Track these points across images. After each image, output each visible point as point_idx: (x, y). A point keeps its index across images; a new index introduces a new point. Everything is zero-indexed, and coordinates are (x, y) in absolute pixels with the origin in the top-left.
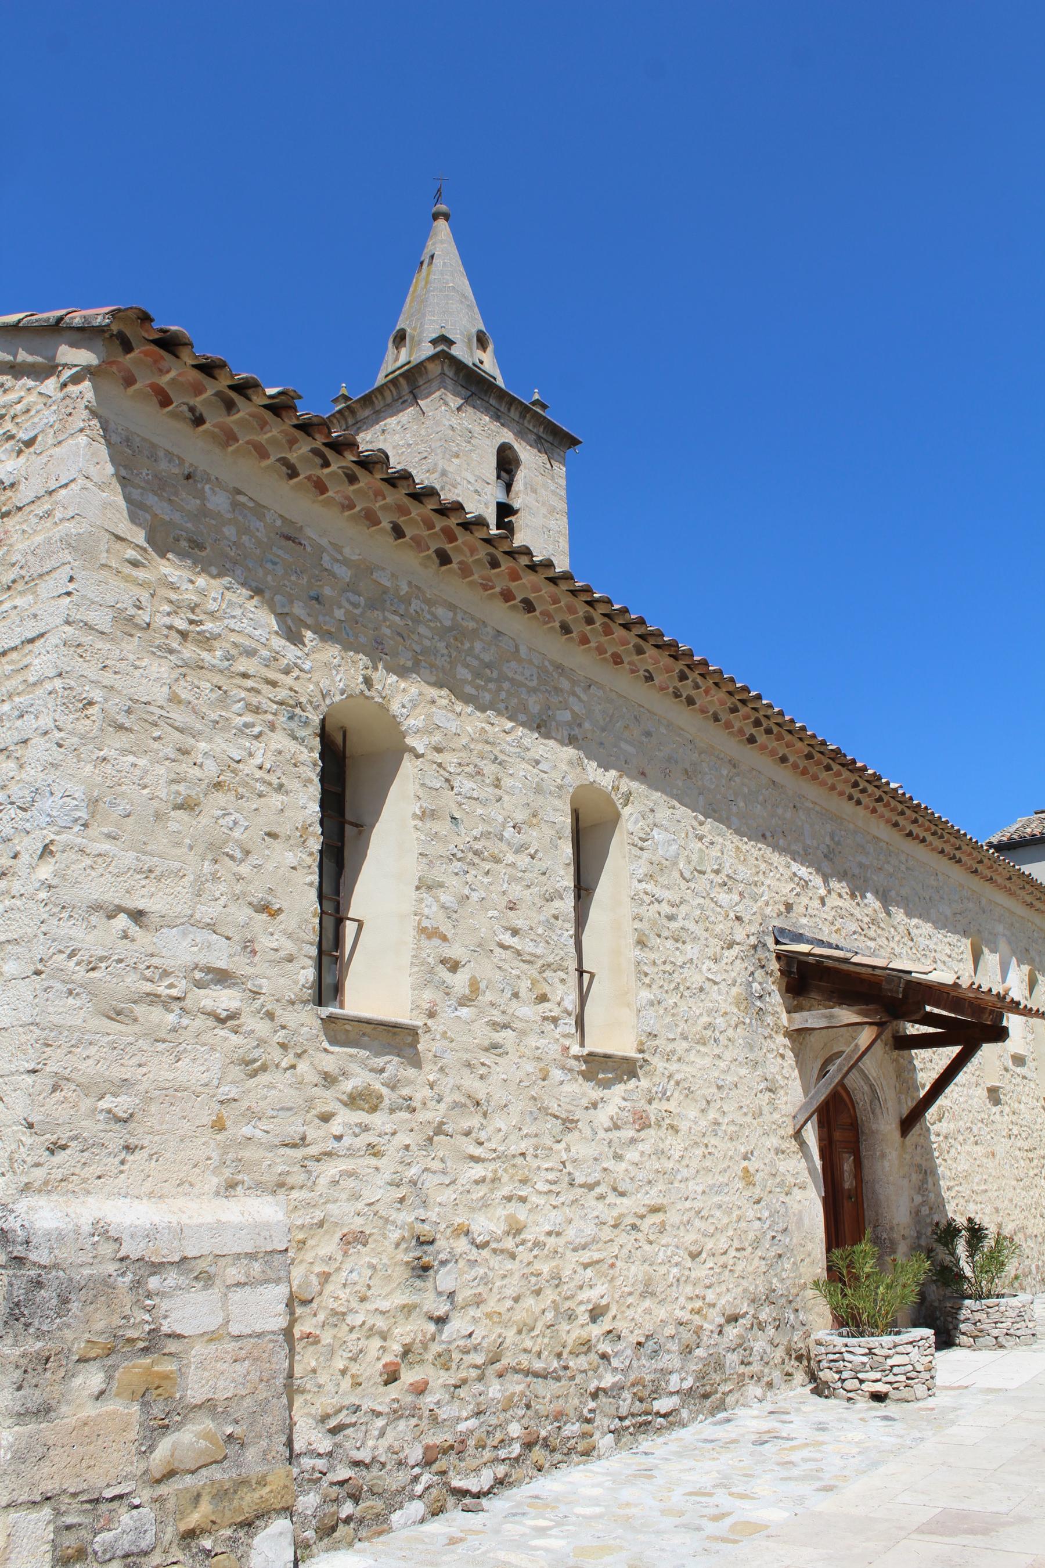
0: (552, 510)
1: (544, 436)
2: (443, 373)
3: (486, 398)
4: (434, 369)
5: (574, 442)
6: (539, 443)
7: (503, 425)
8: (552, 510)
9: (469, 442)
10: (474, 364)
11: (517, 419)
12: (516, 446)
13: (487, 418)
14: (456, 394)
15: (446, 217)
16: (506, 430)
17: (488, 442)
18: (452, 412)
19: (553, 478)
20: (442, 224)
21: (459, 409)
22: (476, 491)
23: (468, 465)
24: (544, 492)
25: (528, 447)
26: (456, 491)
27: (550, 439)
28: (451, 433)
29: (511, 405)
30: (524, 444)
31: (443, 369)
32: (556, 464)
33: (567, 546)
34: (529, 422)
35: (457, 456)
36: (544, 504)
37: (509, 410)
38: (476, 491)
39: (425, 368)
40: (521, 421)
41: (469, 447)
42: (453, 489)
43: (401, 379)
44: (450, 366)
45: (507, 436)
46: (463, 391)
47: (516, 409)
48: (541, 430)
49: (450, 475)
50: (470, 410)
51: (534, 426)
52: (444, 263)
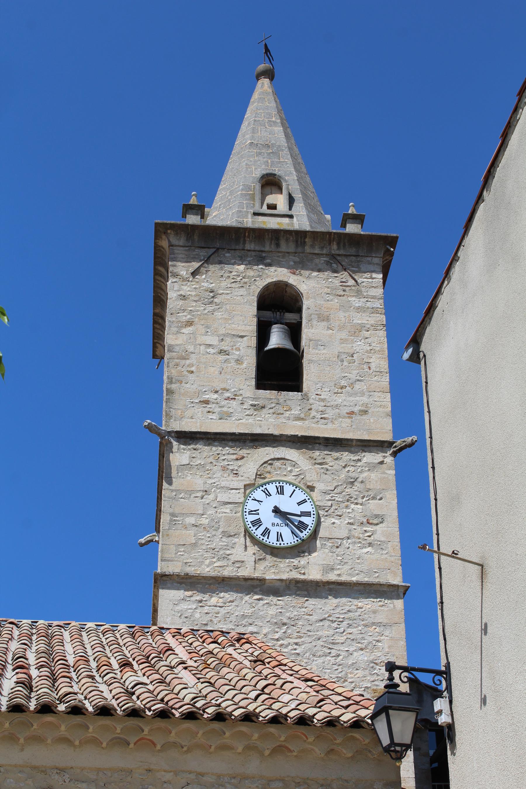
0: (358, 330)
1: (342, 252)
2: (171, 245)
3: (241, 246)
4: (164, 243)
5: (392, 241)
6: (334, 264)
7: (270, 265)
8: (358, 330)
9: (211, 302)
10: (255, 214)
11: (292, 248)
12: (292, 280)
13: (242, 267)
14: (188, 260)
15: (269, 74)
16: (272, 269)
17: (242, 291)
18: (185, 280)
19: (359, 294)
20: (264, 84)
21: (194, 274)
22: (221, 352)
23: (207, 327)
24: (341, 314)
25: (315, 274)
26: (188, 362)
27: (353, 251)
28: (181, 303)
29: (278, 239)
30: (306, 273)
31: (169, 241)
32: (363, 279)
33: (384, 365)
34: (312, 246)
35: (190, 323)
36: (341, 328)
37: (278, 245)
38: (221, 352)
39: (163, 248)
40: (300, 250)
41: (210, 308)
42: (183, 362)
43: (157, 267)
44: (177, 234)
45: (278, 274)
46: (203, 253)
47: (287, 240)
48: (335, 247)
49: (177, 349)
50: (212, 268)
51: (322, 248)
52: (249, 124)
